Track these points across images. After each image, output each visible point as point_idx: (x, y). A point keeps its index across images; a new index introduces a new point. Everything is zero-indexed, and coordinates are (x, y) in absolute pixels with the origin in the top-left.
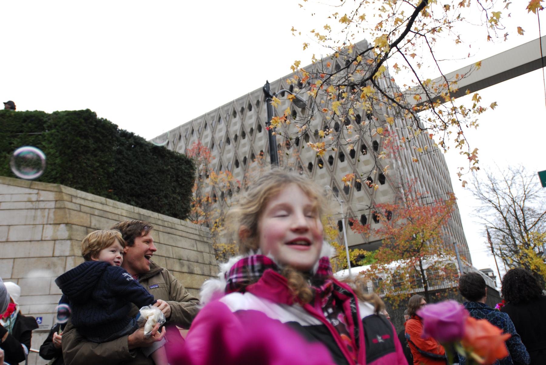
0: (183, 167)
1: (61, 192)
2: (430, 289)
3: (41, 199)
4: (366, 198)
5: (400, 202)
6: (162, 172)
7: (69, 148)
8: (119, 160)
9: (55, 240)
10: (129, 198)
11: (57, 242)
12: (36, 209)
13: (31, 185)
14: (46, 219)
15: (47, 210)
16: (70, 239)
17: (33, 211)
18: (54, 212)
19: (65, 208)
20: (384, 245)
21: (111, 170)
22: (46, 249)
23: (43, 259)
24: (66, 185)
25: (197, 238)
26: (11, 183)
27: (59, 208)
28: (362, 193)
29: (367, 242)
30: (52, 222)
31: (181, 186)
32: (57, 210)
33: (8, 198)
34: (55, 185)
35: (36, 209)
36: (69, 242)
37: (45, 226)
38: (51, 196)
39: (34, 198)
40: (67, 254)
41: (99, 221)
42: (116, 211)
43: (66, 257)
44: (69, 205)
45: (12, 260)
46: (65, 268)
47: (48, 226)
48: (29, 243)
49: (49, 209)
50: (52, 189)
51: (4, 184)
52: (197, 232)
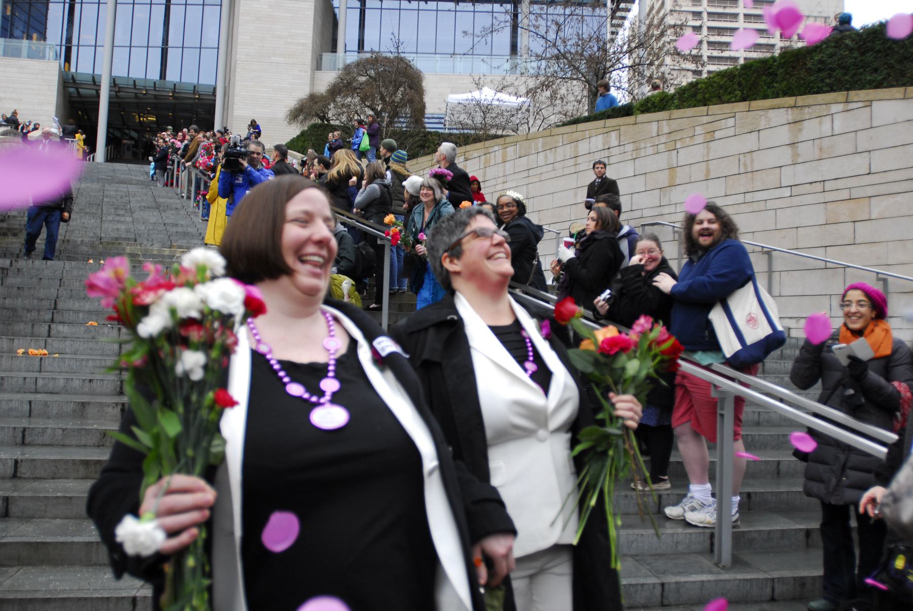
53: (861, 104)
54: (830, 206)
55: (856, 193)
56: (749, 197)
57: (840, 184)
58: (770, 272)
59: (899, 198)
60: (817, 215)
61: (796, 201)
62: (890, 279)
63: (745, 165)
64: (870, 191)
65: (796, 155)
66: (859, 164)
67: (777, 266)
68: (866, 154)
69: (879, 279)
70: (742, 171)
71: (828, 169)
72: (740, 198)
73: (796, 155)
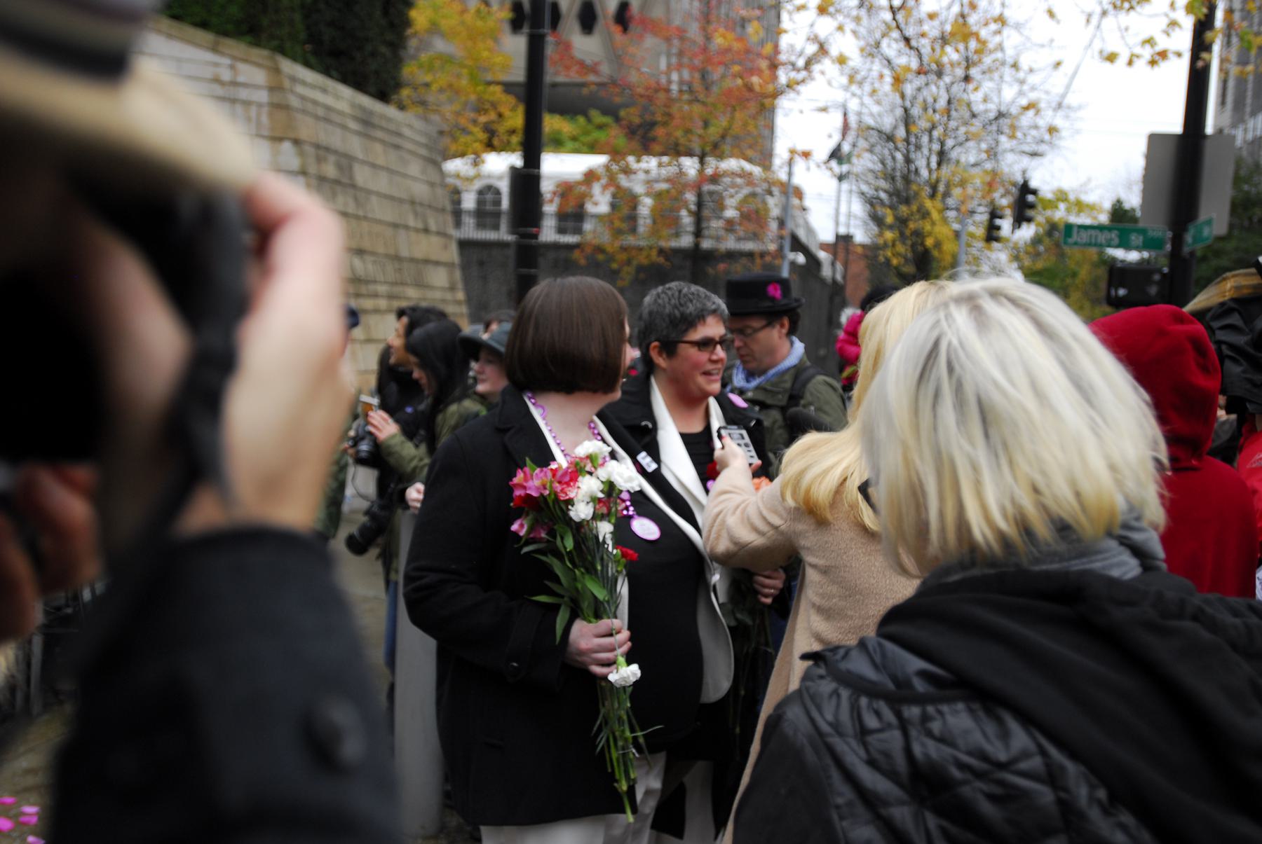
1: (277, 71)
3: (241, 79)
18: (271, 115)
25: (423, 152)
30: (266, 133)
31: (392, 25)
34: (265, 53)
38: (257, 76)
39: (226, 75)
44: (294, 102)
49: (260, 105)
52: (423, 140)
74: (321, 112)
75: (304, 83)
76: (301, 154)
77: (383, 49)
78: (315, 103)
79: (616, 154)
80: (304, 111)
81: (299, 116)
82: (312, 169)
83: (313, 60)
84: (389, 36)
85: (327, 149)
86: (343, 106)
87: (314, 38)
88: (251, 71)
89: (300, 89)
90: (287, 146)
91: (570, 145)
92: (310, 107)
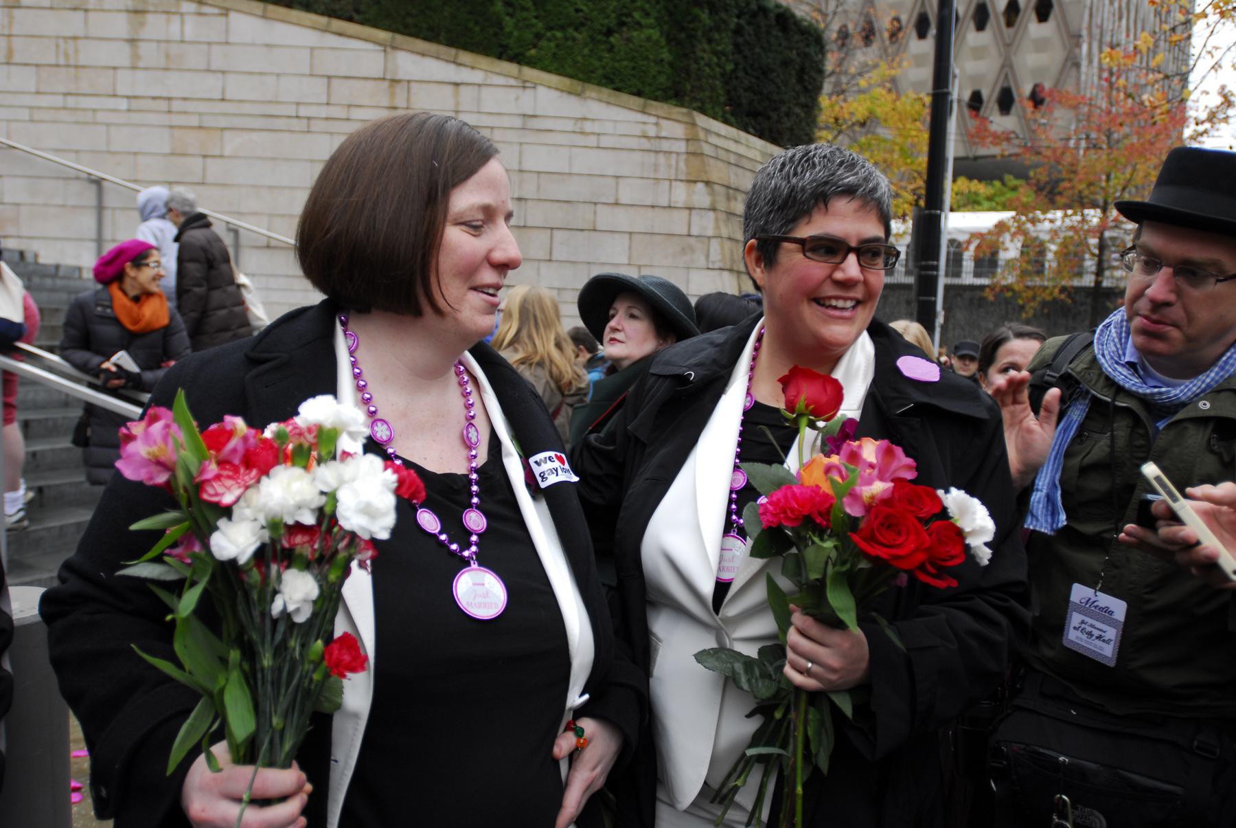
0: (812, 50)
1: (694, 124)
2: (1106, 283)
3: (664, 134)
4: (993, 51)
5: (1074, 72)
6: (786, 63)
7: (683, 29)
8: (738, 48)
9: (690, 209)
10: (746, 119)
11: (694, 212)
12: (657, 152)
13: (645, 106)
14: (673, 171)
15: (674, 156)
16: (714, 209)
17: (652, 155)
18: (687, 160)
19: (702, 154)
20: (1034, 181)
21: (730, 67)
22: (678, 222)
23: (676, 238)
24: (703, 111)
26: (612, 100)
27: (694, 154)
28: (986, 37)
29: (971, 155)
31: (806, 90)
32: (692, 158)
33: (609, 127)
34: (684, 110)
35: (657, 152)
36: (711, 214)
37: (674, 183)
38: (678, 130)
39: (652, 131)
40: (710, 233)
41: (736, 175)
42: (750, 156)
43: (709, 238)
44: (707, 149)
45: (627, 236)
46: (708, 256)
47: (679, 183)
48: (650, 210)
49: (678, 154)
50: (679, 118)
51: (600, 100)
53: (216, 11)
54: (177, 133)
55: (209, 121)
56: (71, 101)
57: (190, 106)
58: (100, 208)
59: (255, 136)
60: (160, 142)
61: (136, 118)
62: (242, 232)
63: (66, 55)
64: (223, 122)
65: (136, 56)
66: (209, 85)
67: (109, 201)
68: (220, 75)
69: (229, 230)
70: (62, 61)
71: (175, 84)
72: (58, 101)
73: (136, 56)
74: (732, 159)
75: (718, 135)
76: (712, 193)
77: (798, 110)
78: (728, 151)
79: (1023, 209)
80: (716, 158)
81: (712, 161)
82: (722, 205)
83: (733, 120)
84: (802, 99)
85: (736, 190)
86: (752, 154)
87: (733, 101)
88: (670, 126)
89: (713, 139)
90: (700, 186)
91: (986, 204)
92: (722, 154)
